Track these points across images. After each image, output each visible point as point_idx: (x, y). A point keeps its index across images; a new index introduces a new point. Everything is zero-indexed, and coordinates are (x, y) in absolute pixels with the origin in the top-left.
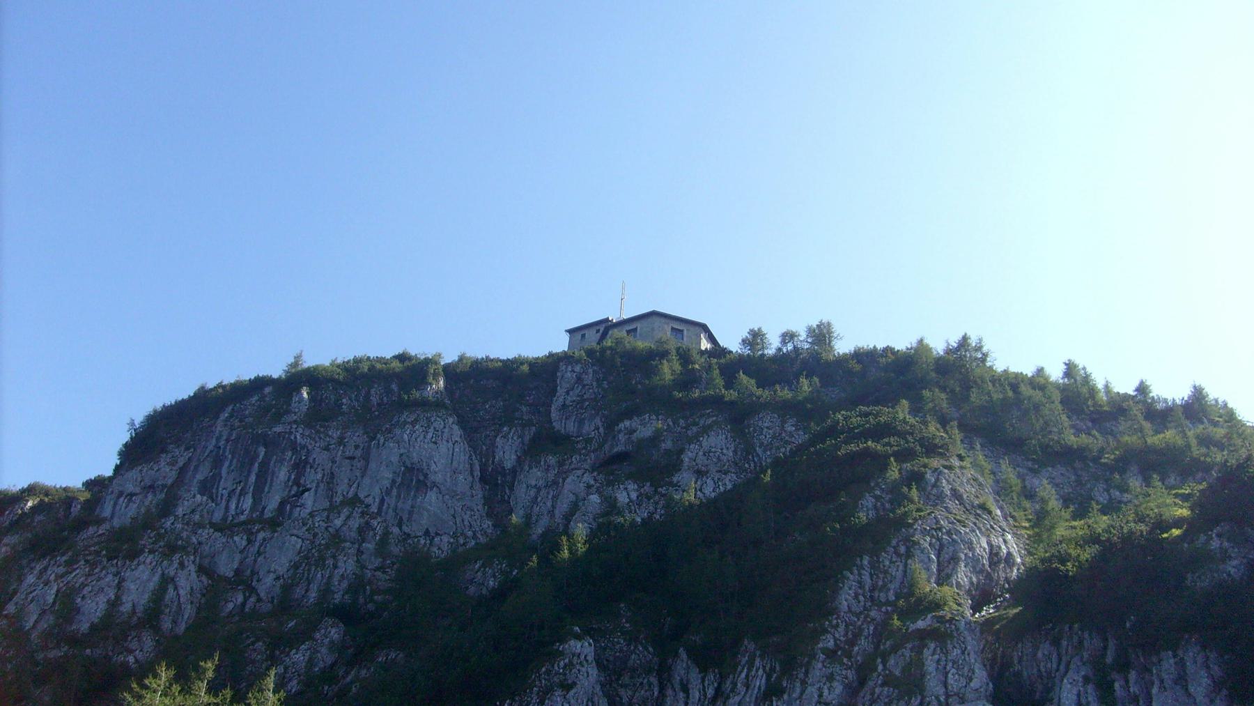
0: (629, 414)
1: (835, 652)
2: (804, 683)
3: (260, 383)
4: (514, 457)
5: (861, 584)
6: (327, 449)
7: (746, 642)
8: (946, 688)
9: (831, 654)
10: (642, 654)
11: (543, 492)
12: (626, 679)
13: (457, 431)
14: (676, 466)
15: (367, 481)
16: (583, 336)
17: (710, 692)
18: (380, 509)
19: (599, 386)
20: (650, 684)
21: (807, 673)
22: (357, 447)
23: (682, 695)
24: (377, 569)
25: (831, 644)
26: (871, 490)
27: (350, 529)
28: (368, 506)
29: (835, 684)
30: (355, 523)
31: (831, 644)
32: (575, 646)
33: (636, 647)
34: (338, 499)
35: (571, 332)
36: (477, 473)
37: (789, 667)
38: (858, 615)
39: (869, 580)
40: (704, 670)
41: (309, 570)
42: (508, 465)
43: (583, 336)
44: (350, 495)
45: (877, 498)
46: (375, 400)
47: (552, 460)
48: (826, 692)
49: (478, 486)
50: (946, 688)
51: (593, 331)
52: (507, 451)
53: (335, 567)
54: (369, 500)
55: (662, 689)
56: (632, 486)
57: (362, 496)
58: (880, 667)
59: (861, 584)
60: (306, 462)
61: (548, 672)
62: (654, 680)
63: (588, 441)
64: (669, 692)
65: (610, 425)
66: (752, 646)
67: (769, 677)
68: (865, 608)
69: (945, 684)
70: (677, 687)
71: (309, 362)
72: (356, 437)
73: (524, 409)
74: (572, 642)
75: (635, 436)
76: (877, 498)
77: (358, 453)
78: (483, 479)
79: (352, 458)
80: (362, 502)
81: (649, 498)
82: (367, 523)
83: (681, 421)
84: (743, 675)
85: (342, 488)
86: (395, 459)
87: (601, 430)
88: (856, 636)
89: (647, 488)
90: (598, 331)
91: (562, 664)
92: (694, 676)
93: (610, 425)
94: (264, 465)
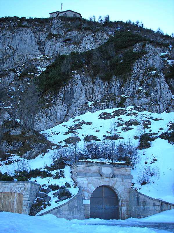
0: (70, 30)
2: (129, 85)
5: (137, 66)
6: (3, 35)
8: (161, 87)
10: (88, 79)
11: (52, 46)
13: (32, 33)
14: (81, 42)
15: (13, 42)
16: (53, 15)
17: (107, 86)
18: (16, 49)
19: (62, 24)
22: (10, 35)
23: (99, 87)
24: (18, 61)
26: (135, 47)
29: (136, 85)
30: (11, 51)
32: (76, 76)
35: (50, 14)
36: (36, 42)
37: (125, 81)
40: (104, 82)
41: (3, 61)
42: (43, 40)
43: (53, 15)
45: (137, 49)
46: (12, 25)
47: (53, 40)
48: (135, 87)
49: (37, 44)
50: (161, 87)
51: (55, 14)
52: (43, 37)
53: (9, 60)
54: (14, 47)
56: (73, 45)
58: (145, 82)
59: (137, 66)
61: (72, 81)
64: (95, 86)
65: (66, 33)
66: (115, 77)
67: (121, 84)
69: (160, 86)
70: (97, 85)
72: (9, 33)
73: (45, 29)
74: (76, 75)
75: (71, 35)
76: (137, 49)
77: (10, 37)
78: (38, 43)
79: (9, 38)
80: (12, 47)
81: (76, 48)
82: (14, 52)
83: (81, 33)
86: (19, 38)
87: (63, 34)
88: (139, 76)
89: (76, 46)
90: (56, 14)
91: (74, 80)
92: (101, 83)
93: (66, 33)
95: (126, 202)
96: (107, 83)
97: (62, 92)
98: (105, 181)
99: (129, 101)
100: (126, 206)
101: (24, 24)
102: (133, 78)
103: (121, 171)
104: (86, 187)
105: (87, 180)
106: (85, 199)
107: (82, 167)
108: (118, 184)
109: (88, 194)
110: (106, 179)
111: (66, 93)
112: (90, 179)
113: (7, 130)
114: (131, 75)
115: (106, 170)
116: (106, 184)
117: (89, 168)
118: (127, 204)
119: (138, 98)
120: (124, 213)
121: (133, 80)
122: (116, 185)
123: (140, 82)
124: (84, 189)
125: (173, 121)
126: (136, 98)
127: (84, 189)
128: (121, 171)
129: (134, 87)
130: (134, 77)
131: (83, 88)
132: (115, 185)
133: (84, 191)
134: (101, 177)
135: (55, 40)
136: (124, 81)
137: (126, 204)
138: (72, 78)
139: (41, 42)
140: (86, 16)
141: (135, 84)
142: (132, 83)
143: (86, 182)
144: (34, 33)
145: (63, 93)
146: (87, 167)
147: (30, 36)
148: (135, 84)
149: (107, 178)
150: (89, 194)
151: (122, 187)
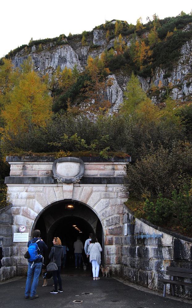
1: (183, 63)
3: (24, 46)
4: (86, 53)
9: (183, 64)
12: (124, 85)
13: (72, 49)
21: (176, 69)
22: (49, 56)
28: (53, 68)
30: (51, 72)
34: (46, 68)
36: (78, 58)
38: (188, 54)
39: (189, 47)
44: (49, 67)
47: (95, 51)
52: (84, 51)
54: (54, 67)
57: (51, 66)
60: (37, 61)
63: (103, 46)
65: (108, 43)
71: (34, 39)
74: (110, 76)
77: (49, 57)
78: (79, 59)
82: (54, 72)
84: (158, 75)
85: (47, 65)
86: (58, 57)
87: (106, 43)
93: (108, 43)
95: (115, 235)
99: (176, 91)
100: (114, 243)
101: (64, 41)
103: (103, 170)
104: (24, 206)
105: (27, 191)
106: (18, 231)
107: (18, 166)
108: (95, 196)
109: (27, 219)
111: (98, 100)
115: (67, 169)
116: (68, 196)
118: (117, 239)
120: (109, 259)
122: (90, 199)
124: (18, 210)
125: (188, 12)
126: (185, 85)
127: (18, 210)
129: (182, 73)
130: (182, 61)
131: (120, 89)
132: (88, 199)
133: (19, 214)
135: (97, 52)
137: (114, 240)
138: (106, 79)
139: (83, 57)
140: (132, 21)
141: (184, 69)
142: (180, 67)
143: (24, 194)
144: (74, 49)
147: (69, 53)
148: (184, 69)
150: (29, 220)
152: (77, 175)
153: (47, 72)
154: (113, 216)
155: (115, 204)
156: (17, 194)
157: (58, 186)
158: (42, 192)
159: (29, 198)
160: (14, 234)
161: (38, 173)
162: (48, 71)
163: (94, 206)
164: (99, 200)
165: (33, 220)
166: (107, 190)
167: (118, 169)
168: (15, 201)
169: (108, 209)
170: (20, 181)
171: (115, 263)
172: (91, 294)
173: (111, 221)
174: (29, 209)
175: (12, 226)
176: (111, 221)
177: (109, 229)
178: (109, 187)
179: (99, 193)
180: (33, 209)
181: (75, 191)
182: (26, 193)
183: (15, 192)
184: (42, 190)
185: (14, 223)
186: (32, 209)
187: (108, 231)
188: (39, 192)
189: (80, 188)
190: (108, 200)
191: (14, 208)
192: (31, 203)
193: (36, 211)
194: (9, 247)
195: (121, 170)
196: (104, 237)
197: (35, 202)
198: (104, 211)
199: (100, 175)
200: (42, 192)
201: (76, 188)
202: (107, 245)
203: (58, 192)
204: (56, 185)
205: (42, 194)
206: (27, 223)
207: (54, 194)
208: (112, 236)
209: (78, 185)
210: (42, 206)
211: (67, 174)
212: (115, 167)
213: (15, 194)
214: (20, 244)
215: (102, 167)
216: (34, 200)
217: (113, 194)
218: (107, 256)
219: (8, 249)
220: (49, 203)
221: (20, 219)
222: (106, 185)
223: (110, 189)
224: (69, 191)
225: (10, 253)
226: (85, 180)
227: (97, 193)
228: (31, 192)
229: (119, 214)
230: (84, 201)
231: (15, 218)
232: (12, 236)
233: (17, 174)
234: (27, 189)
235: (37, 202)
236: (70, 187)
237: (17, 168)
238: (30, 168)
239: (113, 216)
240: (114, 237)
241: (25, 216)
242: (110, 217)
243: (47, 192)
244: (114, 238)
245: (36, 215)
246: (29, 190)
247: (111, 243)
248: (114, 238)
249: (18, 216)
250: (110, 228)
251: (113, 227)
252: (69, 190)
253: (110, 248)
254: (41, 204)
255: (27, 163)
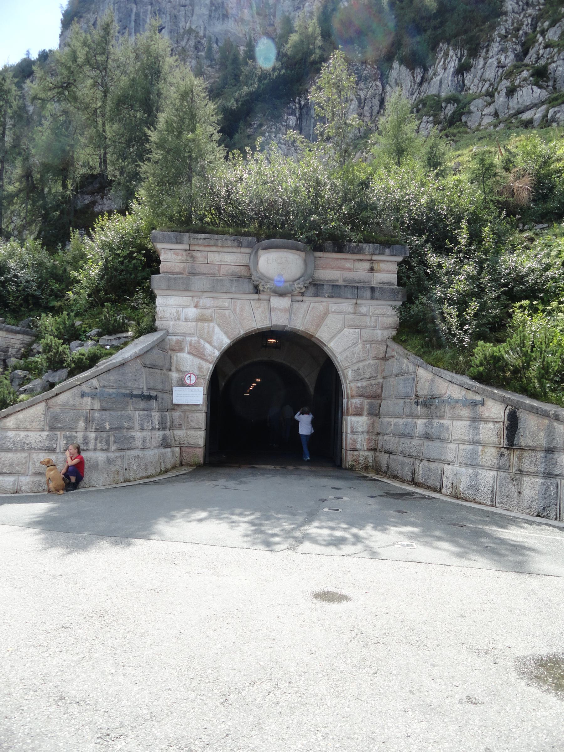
1: (506, 37)
7: (441, 45)
9: (504, 37)
17: (418, 79)
20: (377, 86)
21: (487, 51)
25: (503, 32)
27: (190, 47)
30: (192, 43)
31: (503, 32)
33: (366, 66)
34: (182, 31)
36: (254, 9)
37: (474, 52)
44: (187, 28)
55: (384, 87)
57: (193, 27)
62: (379, 83)
64: (388, 88)
66: (446, 46)
67: (460, 60)
68: (523, 10)
80: (194, 31)
82: (199, 42)
84: (441, 63)
85: (182, 24)
94: (137, 15)
96: (419, 72)
97: (293, 113)
98: (276, 309)
102: (500, 35)
103: (350, 270)
104: (191, 335)
105: (196, 306)
106: (182, 383)
107: (177, 254)
108: (333, 322)
109: (197, 361)
110: (278, 302)
112: (207, 301)
113: (88, 199)
114: (493, 28)
117: (206, 257)
118: (371, 406)
119: (511, 92)
121: (498, 39)
122: (323, 328)
123: (523, 45)
128: (350, 270)
132: (318, 326)
133: (181, 350)
134: (257, 293)
136: (469, 50)
137: (366, 407)
142: (495, 47)
143: (192, 312)
145: (295, 115)
146: (198, 255)
149: (282, 294)
151: (350, 334)
152: (299, 279)
153: (183, 43)
154: (367, 363)
155: (371, 340)
156: (177, 312)
157: (259, 299)
158: (227, 308)
159: (201, 319)
160: (175, 389)
161: (219, 270)
162: (185, 40)
163: (330, 341)
164: (341, 330)
165: (210, 363)
166: (358, 311)
167: (379, 271)
168: (174, 325)
169: (357, 348)
170: (182, 283)
171: (365, 448)
172: (345, 498)
173: (361, 371)
174: (202, 342)
175: (170, 373)
176: (361, 371)
177: (358, 387)
178: (361, 305)
179: (340, 316)
180: (210, 343)
181: (294, 310)
182: (195, 310)
183: (172, 306)
184: (226, 304)
185: (173, 368)
186: (207, 342)
187: (354, 389)
188: (221, 308)
189: (304, 306)
190: (357, 330)
191: (172, 340)
192: (206, 331)
193: (217, 345)
194: (167, 414)
195: (388, 272)
196: (345, 401)
197: (213, 328)
198: (348, 353)
199: (345, 281)
200: (227, 308)
201: (296, 305)
202: (351, 415)
203: (260, 310)
204: (256, 296)
205: (227, 312)
206: (200, 368)
207: (256, 316)
208: (362, 399)
209: (300, 298)
210: (229, 337)
211: (280, 275)
212: (375, 266)
213: (174, 310)
214: (186, 408)
215: (348, 265)
216: (211, 324)
217: (368, 319)
218: (350, 436)
219: (166, 416)
220: (242, 333)
221: (186, 360)
222: (354, 301)
223: (364, 310)
224: (281, 310)
225: (169, 424)
226: (315, 287)
227: (337, 316)
228: (205, 307)
229: (378, 359)
230: (311, 331)
231: (175, 358)
232: (171, 392)
233: (175, 271)
234: (198, 302)
235: (217, 329)
236: (285, 302)
237: (174, 256)
238: (201, 259)
239: (367, 363)
240: (366, 401)
241: (194, 355)
242: (361, 365)
243: (238, 311)
244: (366, 404)
245: (217, 354)
246: (201, 304)
247: (359, 414)
248: (366, 404)
249: (179, 354)
250: (359, 384)
251: (365, 384)
252: (282, 307)
253: (358, 422)
254: (226, 333)
255: (196, 248)
